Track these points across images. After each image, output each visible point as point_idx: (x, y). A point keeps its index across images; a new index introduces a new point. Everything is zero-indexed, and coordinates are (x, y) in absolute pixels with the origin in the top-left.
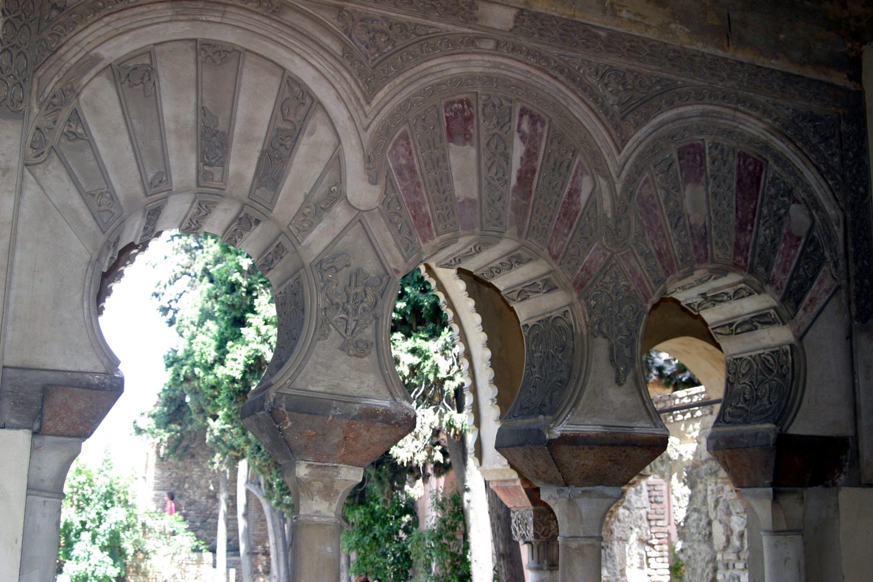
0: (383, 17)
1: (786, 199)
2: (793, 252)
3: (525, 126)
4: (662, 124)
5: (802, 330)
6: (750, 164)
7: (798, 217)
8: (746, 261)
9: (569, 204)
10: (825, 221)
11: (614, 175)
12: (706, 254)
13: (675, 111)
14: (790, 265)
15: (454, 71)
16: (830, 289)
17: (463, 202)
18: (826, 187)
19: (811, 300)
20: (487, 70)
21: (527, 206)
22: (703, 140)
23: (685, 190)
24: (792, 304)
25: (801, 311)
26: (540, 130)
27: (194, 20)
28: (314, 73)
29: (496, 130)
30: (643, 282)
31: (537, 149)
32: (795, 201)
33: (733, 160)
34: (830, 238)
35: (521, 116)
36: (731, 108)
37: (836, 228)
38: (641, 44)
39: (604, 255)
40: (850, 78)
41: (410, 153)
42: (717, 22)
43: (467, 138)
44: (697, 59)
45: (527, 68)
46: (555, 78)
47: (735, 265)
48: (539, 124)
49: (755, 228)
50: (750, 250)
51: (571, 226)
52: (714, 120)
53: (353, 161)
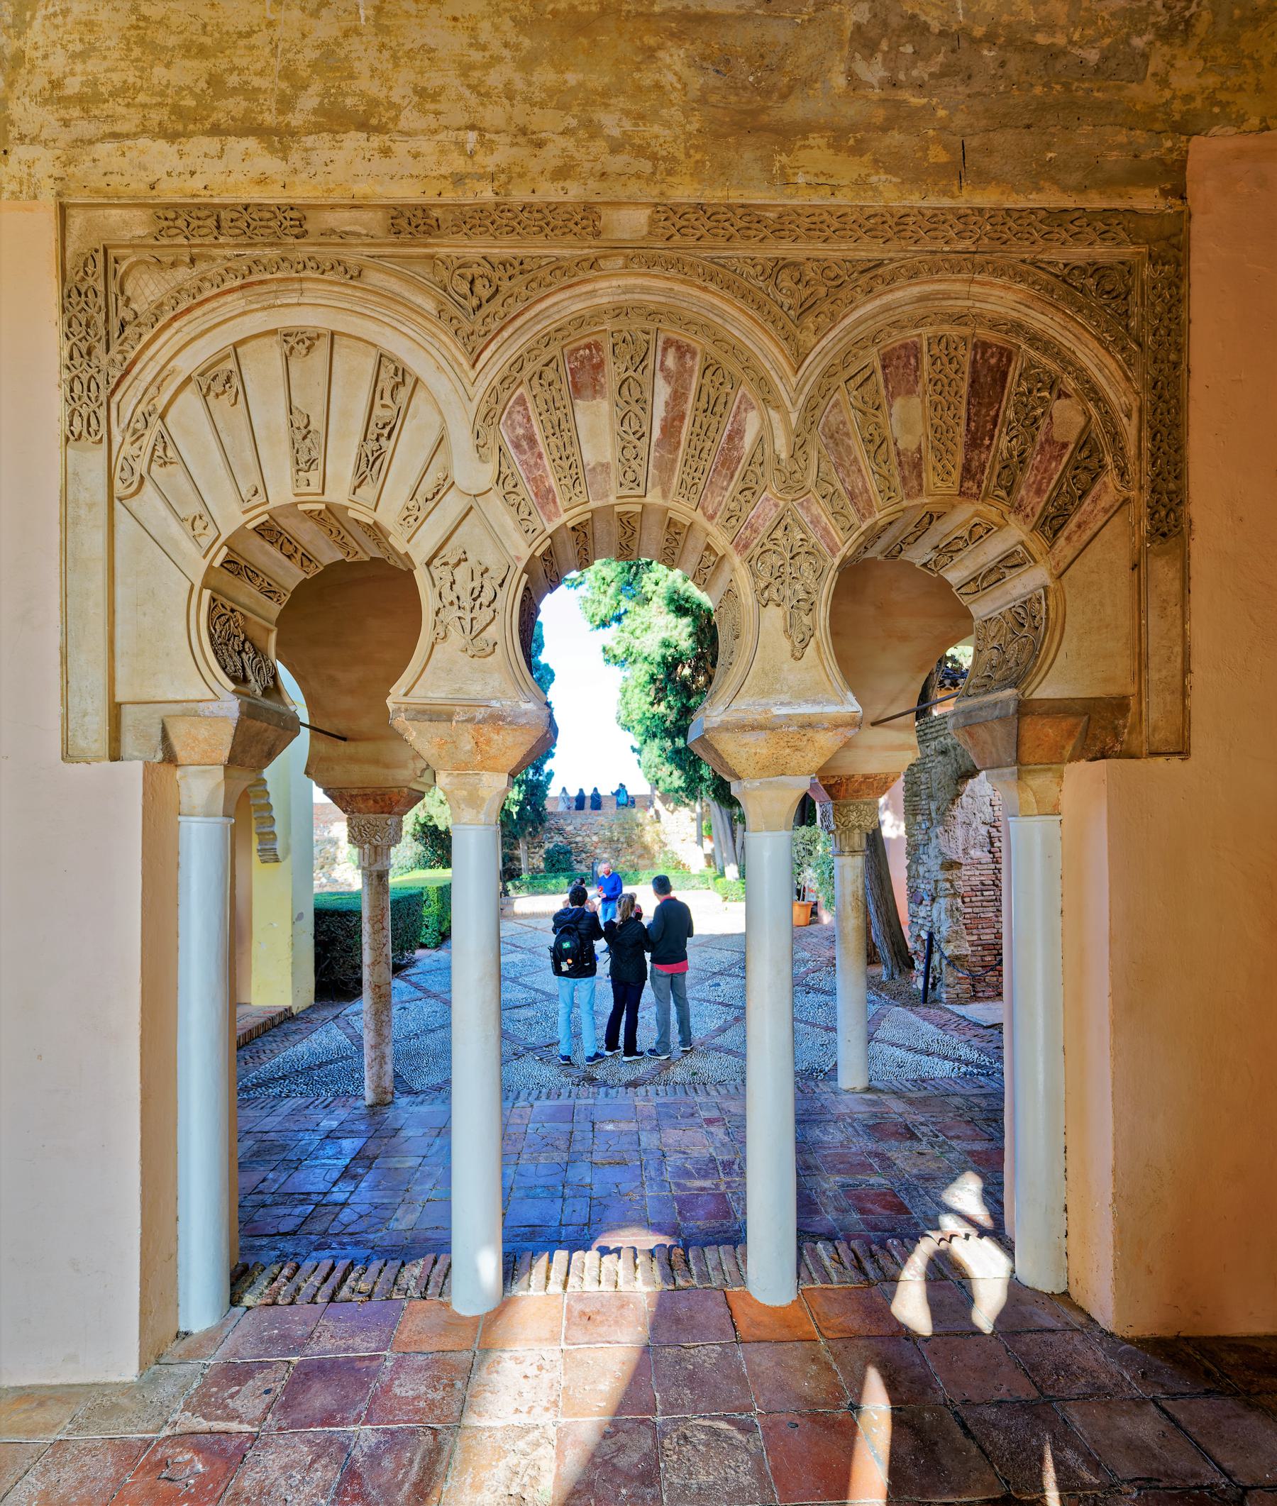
0: (484, 258)
1: (1046, 394)
2: (1054, 464)
3: (671, 362)
4: (859, 322)
5: (1063, 566)
6: (992, 356)
7: (1067, 417)
8: (979, 486)
9: (729, 450)
10: (1108, 416)
11: (788, 403)
12: (921, 485)
13: (878, 302)
14: (1049, 482)
15: (574, 308)
16: (1111, 507)
17: (594, 469)
18: (1113, 366)
19: (1079, 526)
20: (616, 298)
21: (674, 461)
22: (920, 335)
23: (891, 406)
24: (1049, 533)
25: (1061, 542)
26: (689, 363)
29: (630, 373)
30: (829, 533)
31: (687, 388)
32: (1062, 394)
33: (966, 356)
34: (1115, 436)
35: (665, 350)
36: (964, 281)
37: (1125, 420)
38: (825, 216)
39: (776, 505)
40: (1165, 193)
41: (529, 420)
42: (944, 158)
43: (596, 390)
44: (910, 220)
45: (669, 285)
46: (705, 289)
47: (961, 493)
48: (688, 355)
49: (995, 442)
50: (987, 471)
51: (732, 477)
52: (936, 303)
53: (461, 438)
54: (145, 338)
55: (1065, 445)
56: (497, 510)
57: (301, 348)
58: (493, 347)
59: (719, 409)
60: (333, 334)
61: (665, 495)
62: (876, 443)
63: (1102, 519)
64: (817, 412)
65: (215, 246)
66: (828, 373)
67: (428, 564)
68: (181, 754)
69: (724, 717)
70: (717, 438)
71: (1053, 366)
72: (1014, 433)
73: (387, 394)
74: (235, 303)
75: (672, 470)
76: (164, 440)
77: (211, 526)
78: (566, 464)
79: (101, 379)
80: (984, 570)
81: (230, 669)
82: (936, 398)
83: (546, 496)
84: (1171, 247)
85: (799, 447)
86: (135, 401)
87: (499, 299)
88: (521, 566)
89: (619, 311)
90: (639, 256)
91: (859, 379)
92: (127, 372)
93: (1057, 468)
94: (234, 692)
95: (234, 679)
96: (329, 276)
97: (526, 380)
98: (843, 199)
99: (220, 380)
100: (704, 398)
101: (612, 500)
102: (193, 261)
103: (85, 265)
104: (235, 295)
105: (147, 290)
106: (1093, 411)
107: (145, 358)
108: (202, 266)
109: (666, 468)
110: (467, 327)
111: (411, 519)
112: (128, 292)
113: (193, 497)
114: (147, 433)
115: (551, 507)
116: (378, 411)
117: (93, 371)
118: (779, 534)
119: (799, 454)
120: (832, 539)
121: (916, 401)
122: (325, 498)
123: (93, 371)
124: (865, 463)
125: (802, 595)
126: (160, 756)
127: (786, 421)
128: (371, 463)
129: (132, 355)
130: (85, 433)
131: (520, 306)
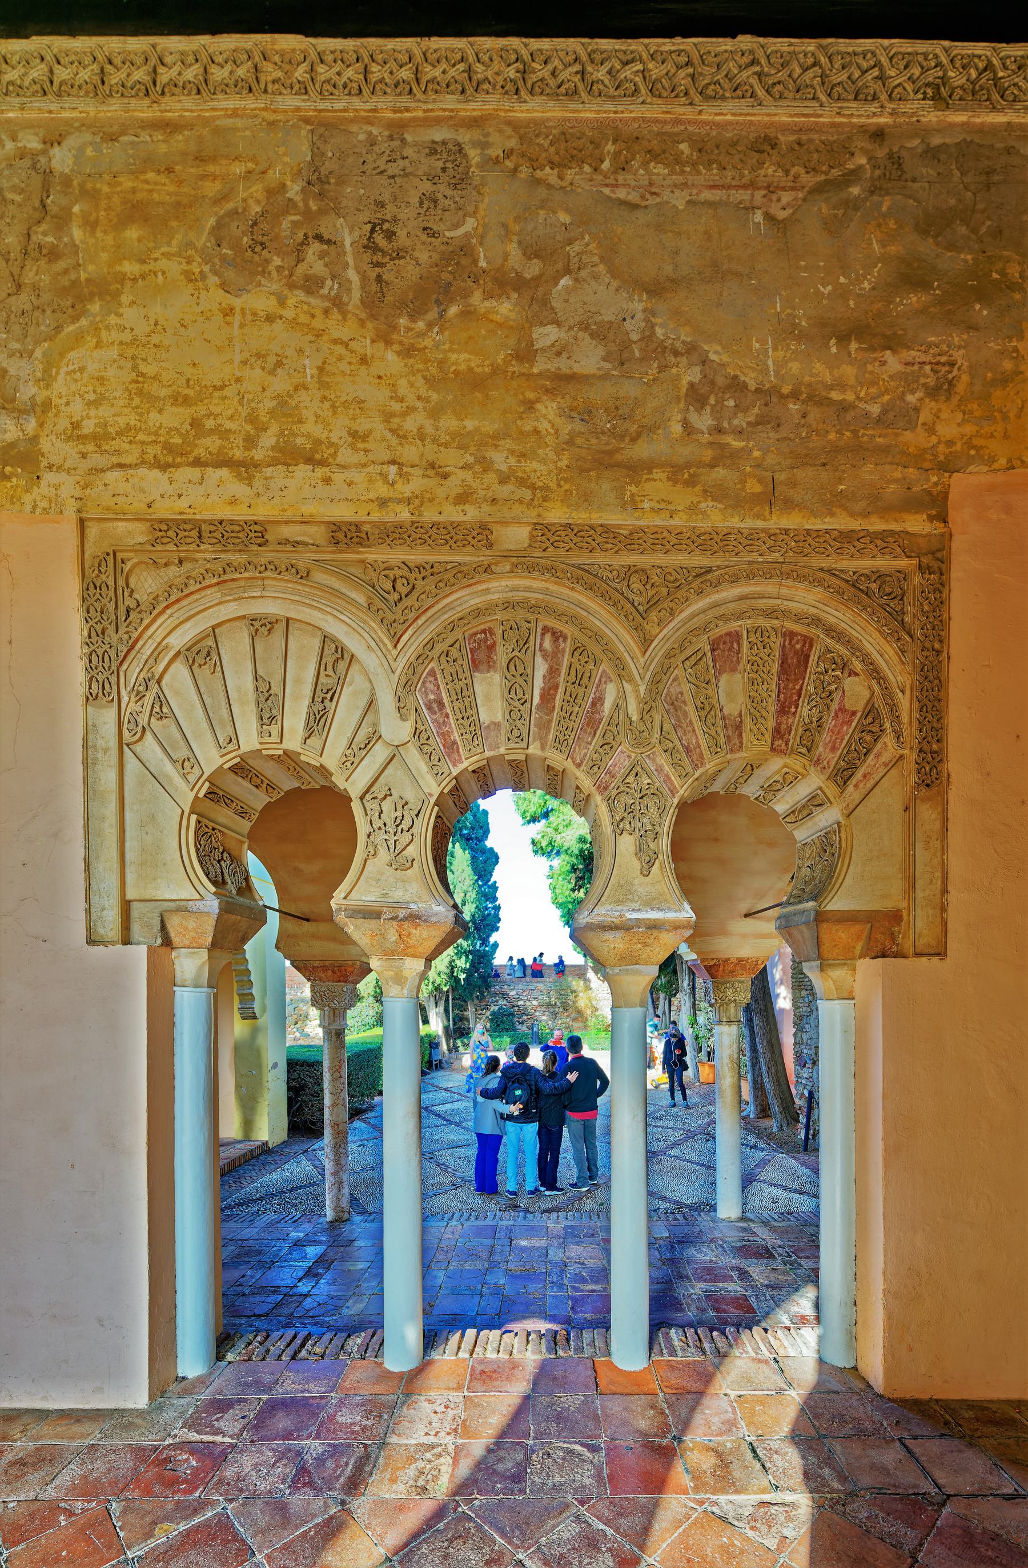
1: (839, 673)
3: (547, 644)
5: (851, 807)
7: (856, 691)
10: (886, 689)
17: (488, 727)
21: (550, 721)
23: (718, 681)
25: (851, 788)
26: (562, 645)
27: (240, 598)
28: (345, 628)
31: (560, 665)
32: (853, 673)
34: (893, 708)
35: (543, 635)
37: (900, 694)
39: (629, 757)
41: (438, 688)
43: (490, 665)
53: (386, 701)
54: (146, 622)
55: (854, 713)
56: (414, 757)
57: (264, 630)
58: (410, 631)
59: (585, 681)
60: (288, 619)
61: (543, 748)
62: (706, 709)
63: (882, 771)
64: (661, 686)
65: (198, 552)
66: (669, 655)
67: (362, 798)
68: (176, 939)
69: (588, 920)
70: (583, 704)
71: (844, 651)
72: (814, 703)
73: (330, 667)
74: (213, 595)
75: (549, 728)
76: (161, 700)
77: (196, 769)
78: (466, 723)
79: (112, 653)
80: (799, 806)
81: (212, 875)
82: (753, 675)
83: (451, 747)
84: (936, 561)
85: (646, 712)
86: (138, 670)
87: (415, 595)
88: (433, 800)
89: (508, 605)
90: (523, 563)
91: (693, 660)
92: (132, 647)
93: (848, 731)
94: (215, 894)
95: (215, 883)
96: (285, 576)
97: (436, 656)
98: (679, 521)
99: (202, 654)
100: (573, 673)
101: (502, 751)
102: (180, 562)
103: (100, 565)
104: (213, 589)
105: (147, 584)
106: (876, 687)
107: (145, 637)
108: (187, 566)
109: (544, 726)
110: (391, 617)
111: (348, 764)
112: (132, 585)
113: (182, 743)
114: (148, 694)
115: (455, 755)
116: (323, 679)
117: (106, 647)
118: (631, 779)
119: (646, 717)
120: (672, 783)
121: (738, 677)
122: (284, 746)
123: (106, 647)
124: (697, 725)
125: (649, 827)
126: (159, 941)
127: (637, 692)
128: (318, 720)
129: (135, 635)
130: (100, 694)
131: (430, 601)
